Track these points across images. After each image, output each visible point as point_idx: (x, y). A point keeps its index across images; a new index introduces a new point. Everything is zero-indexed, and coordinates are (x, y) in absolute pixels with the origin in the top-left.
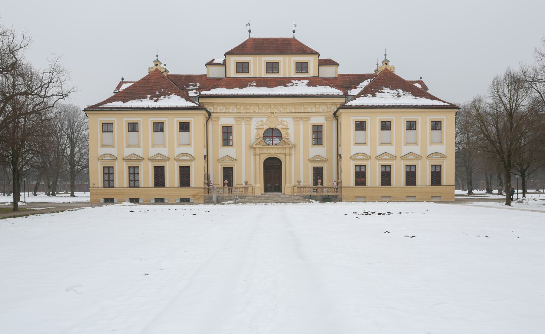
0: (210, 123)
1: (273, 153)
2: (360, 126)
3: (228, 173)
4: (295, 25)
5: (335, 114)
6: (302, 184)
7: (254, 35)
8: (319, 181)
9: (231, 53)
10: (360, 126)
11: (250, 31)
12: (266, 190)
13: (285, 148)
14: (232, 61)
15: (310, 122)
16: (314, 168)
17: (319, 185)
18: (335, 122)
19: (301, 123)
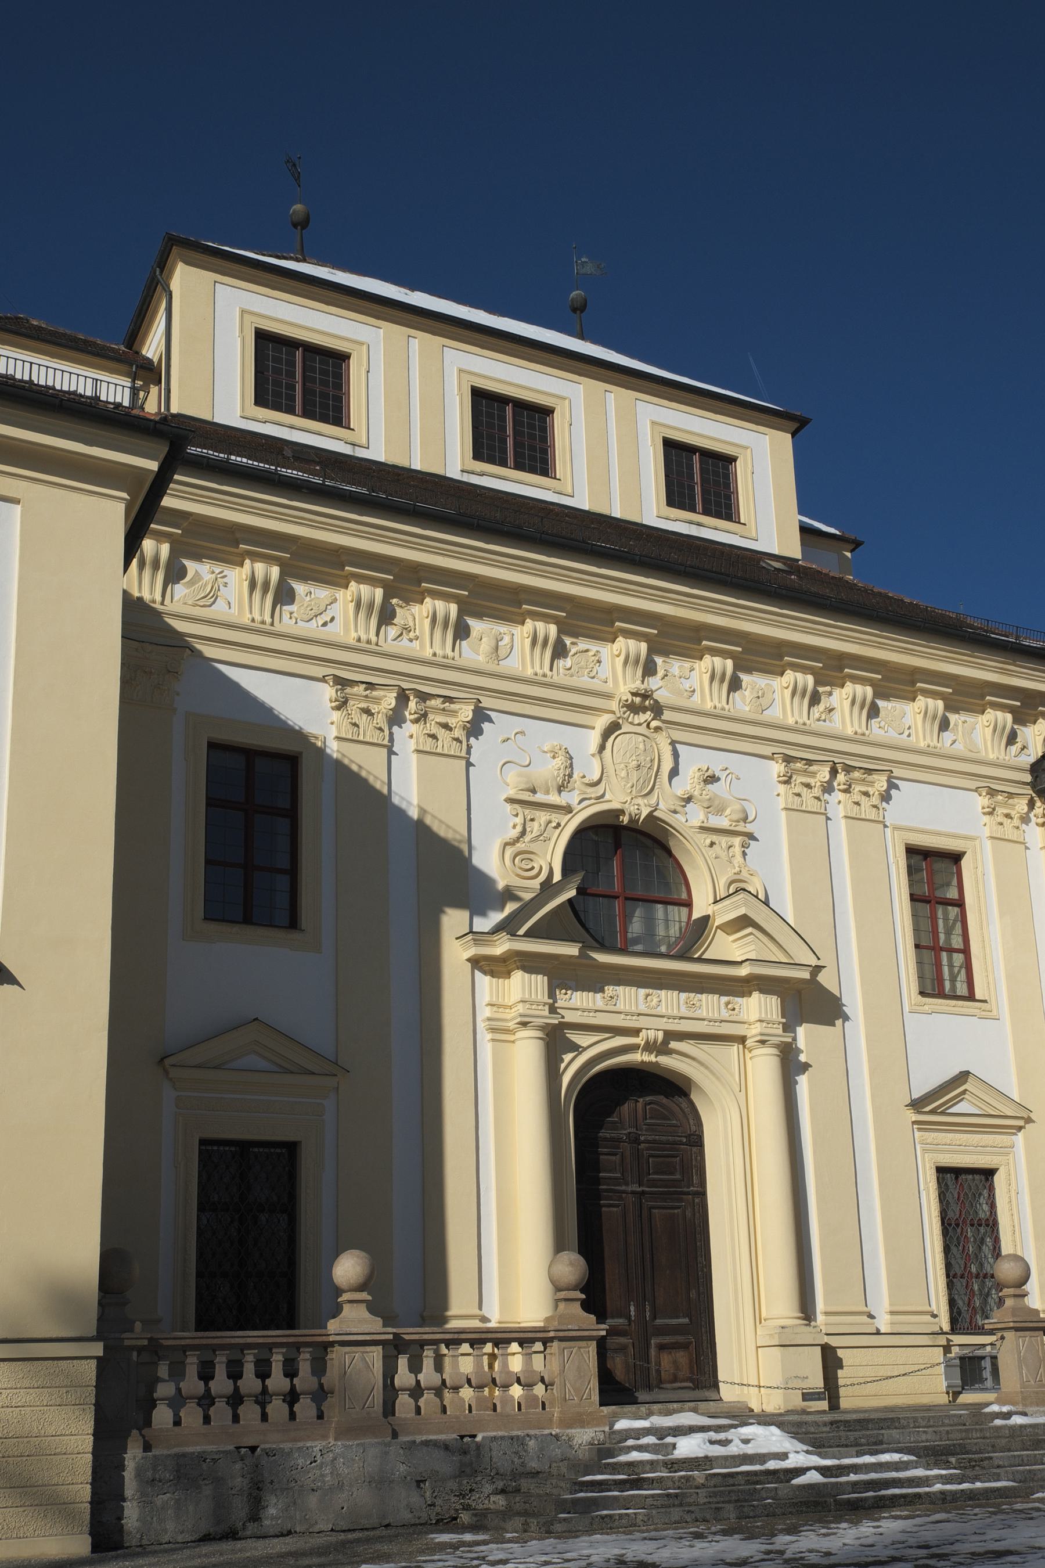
15: (895, 812)
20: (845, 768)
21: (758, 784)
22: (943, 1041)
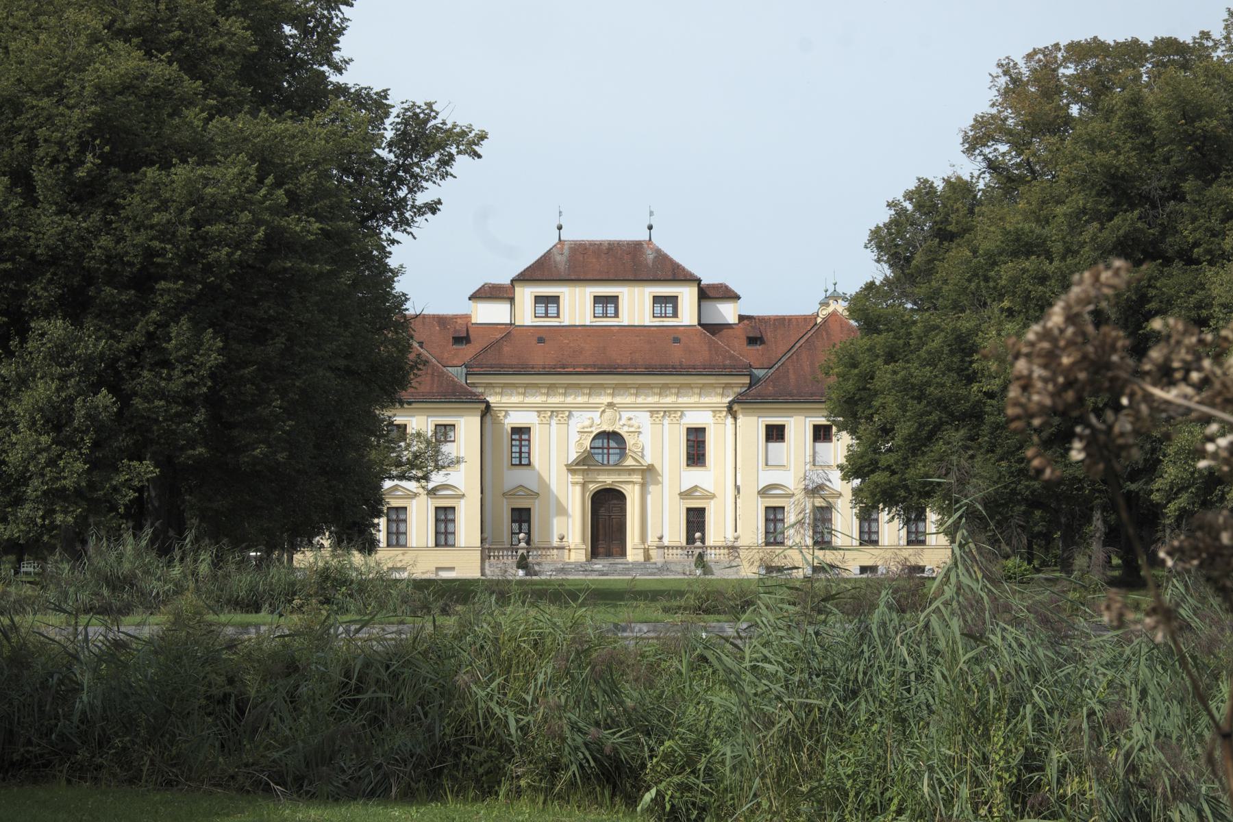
0: (488, 419)
2: (775, 433)
4: (651, 213)
5: (730, 409)
6: (666, 542)
7: (567, 235)
9: (527, 277)
10: (775, 433)
11: (560, 228)
14: (525, 295)
16: (689, 510)
17: (698, 544)
18: (730, 420)
19: (666, 421)
21: (643, 419)
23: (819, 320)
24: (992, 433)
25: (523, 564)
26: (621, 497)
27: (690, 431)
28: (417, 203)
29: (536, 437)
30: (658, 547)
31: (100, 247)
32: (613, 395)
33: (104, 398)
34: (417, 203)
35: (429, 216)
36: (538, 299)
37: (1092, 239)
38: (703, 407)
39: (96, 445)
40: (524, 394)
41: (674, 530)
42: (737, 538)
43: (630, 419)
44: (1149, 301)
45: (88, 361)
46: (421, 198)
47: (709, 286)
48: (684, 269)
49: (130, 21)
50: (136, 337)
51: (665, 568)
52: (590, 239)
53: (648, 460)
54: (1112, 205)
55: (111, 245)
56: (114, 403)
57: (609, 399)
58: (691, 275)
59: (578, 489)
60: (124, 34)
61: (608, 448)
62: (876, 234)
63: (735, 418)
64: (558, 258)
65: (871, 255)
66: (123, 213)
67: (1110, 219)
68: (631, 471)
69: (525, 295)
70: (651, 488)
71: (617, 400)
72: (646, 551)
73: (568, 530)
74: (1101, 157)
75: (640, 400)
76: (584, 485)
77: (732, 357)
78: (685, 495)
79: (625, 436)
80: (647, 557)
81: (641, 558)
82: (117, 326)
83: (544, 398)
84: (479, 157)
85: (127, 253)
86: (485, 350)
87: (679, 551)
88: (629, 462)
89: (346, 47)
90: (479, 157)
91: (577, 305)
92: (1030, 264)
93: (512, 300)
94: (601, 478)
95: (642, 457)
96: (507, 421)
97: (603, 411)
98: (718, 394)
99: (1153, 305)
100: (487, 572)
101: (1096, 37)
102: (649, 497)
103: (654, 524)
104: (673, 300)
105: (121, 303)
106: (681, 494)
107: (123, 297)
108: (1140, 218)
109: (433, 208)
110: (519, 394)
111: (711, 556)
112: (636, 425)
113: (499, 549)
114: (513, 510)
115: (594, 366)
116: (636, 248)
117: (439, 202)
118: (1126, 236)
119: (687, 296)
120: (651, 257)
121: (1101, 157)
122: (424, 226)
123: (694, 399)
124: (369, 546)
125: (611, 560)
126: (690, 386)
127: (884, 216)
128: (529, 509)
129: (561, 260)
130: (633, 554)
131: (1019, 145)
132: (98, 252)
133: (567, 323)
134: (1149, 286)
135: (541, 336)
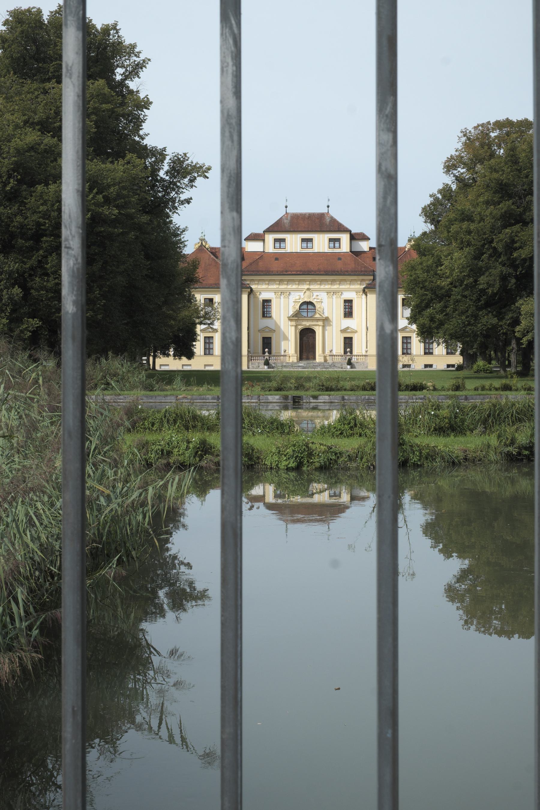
0: (252, 296)
1: (308, 324)
3: (267, 343)
4: (329, 200)
5: (364, 291)
6: (334, 353)
8: (348, 350)
9: (270, 230)
11: (286, 207)
12: (301, 358)
13: (319, 319)
14: (270, 238)
15: (343, 296)
16: (345, 338)
17: (349, 354)
18: (364, 296)
20: (335, 293)
21: (323, 296)
22: (347, 323)
23: (407, 249)
24: (454, 304)
25: (267, 363)
26: (313, 332)
27: (346, 301)
28: (181, 199)
29: (274, 304)
30: (330, 356)
31: (17, 222)
32: (309, 284)
33: (17, 291)
34: (181, 199)
35: (186, 205)
36: (276, 240)
37: (491, 214)
38: (352, 290)
39: (13, 311)
40: (268, 284)
41: (338, 348)
42: (367, 351)
43: (317, 296)
44: (516, 243)
45: (10, 273)
46: (183, 197)
47: (355, 234)
48: (343, 226)
49: (37, 118)
50: (33, 262)
51: (333, 365)
52: (300, 212)
53: (326, 315)
54: (501, 198)
55: (22, 220)
56: (21, 292)
57: (307, 287)
58: (347, 228)
59: (293, 328)
60: (33, 125)
61: (308, 309)
62: (424, 210)
63: (366, 295)
64: (285, 221)
65: (422, 219)
66: (27, 206)
67: (499, 205)
68: (318, 320)
69: (270, 238)
70: (327, 328)
71: (312, 287)
72: (325, 357)
73: (288, 347)
74: (495, 175)
75: (322, 287)
76: (296, 326)
77: (365, 267)
78: (343, 331)
79: (315, 303)
80: (326, 360)
81: (322, 361)
82: (25, 257)
83: (277, 286)
84: (208, 178)
85: (29, 225)
86: (251, 264)
87: (340, 357)
88: (317, 316)
89: (146, 128)
90: (208, 178)
91: (293, 243)
92: (465, 225)
93: (264, 240)
94: (304, 323)
95: (323, 313)
96: (260, 297)
97: (305, 292)
98: (358, 284)
99: (517, 245)
100: (250, 367)
101: (507, 119)
102: (326, 332)
103: (329, 344)
104: (338, 240)
105: (26, 247)
106: (341, 331)
107: (27, 244)
108: (513, 204)
109: (188, 201)
110: (266, 284)
111: (354, 360)
112: (320, 298)
113: (256, 356)
114: (263, 338)
115: (301, 271)
116: (321, 216)
117: (191, 199)
118: (505, 212)
119: (345, 238)
120: (328, 220)
121: (495, 175)
122: (183, 210)
123: (347, 286)
124: (190, 355)
125: (309, 362)
126: (345, 280)
127: (428, 201)
128: (271, 338)
129: (286, 222)
130: (319, 359)
131: (470, 168)
132: (16, 224)
133: (289, 251)
134: (517, 236)
135: (277, 257)
